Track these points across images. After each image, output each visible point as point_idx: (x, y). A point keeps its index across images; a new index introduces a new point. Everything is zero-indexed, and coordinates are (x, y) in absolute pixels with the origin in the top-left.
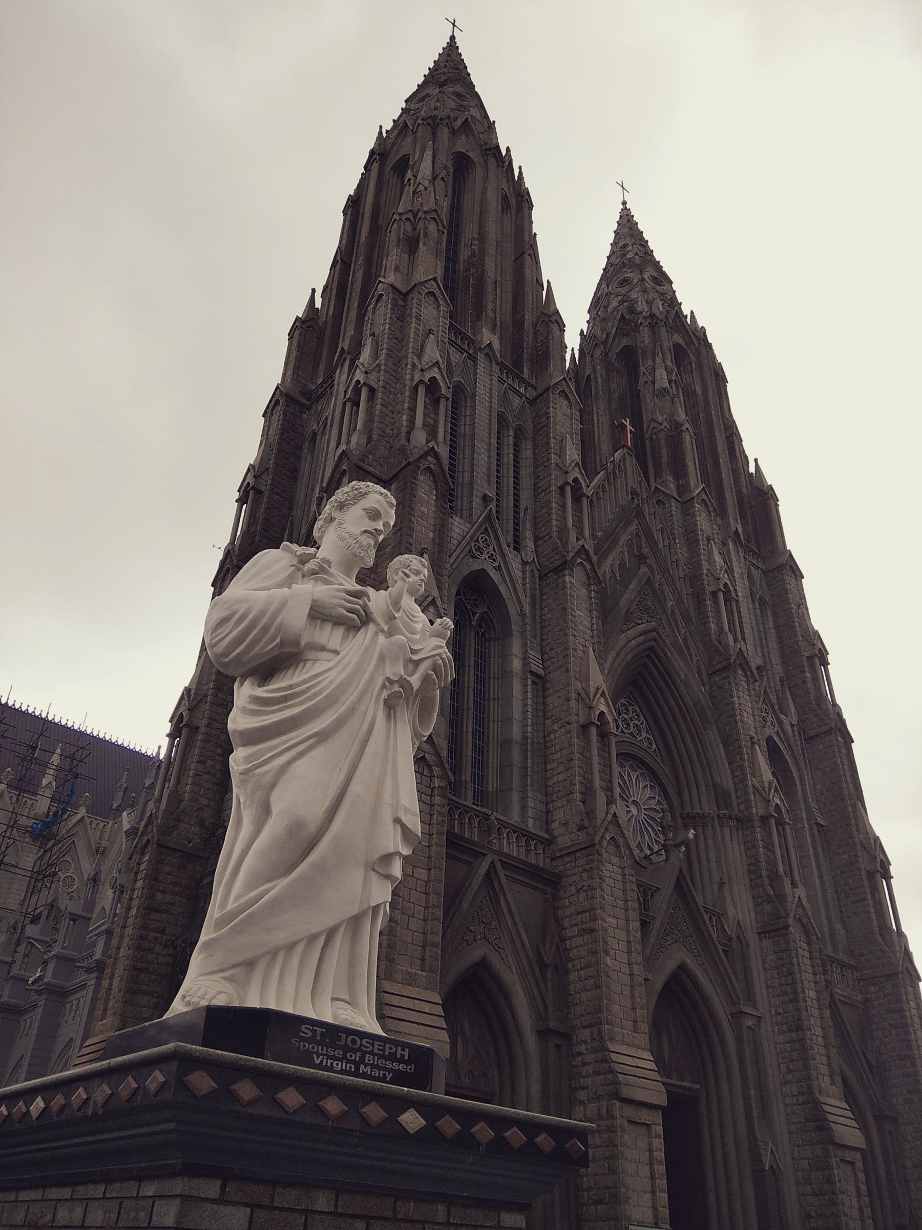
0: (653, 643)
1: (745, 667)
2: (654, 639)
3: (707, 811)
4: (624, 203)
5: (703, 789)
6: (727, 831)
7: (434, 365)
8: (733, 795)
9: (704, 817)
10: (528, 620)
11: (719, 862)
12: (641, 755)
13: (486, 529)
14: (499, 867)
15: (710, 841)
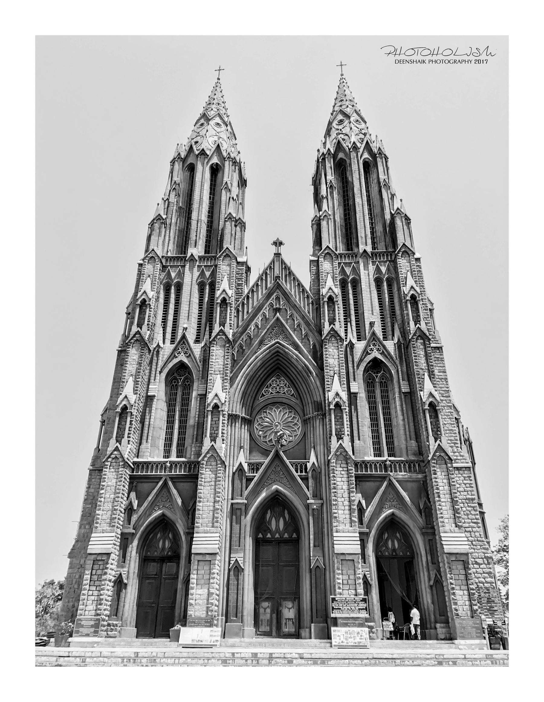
0: (278, 349)
1: (336, 335)
2: (278, 347)
3: (311, 415)
4: (342, 75)
5: (310, 405)
6: (318, 421)
7: (143, 293)
8: (323, 403)
9: (309, 418)
10: (201, 372)
11: (314, 437)
12: (280, 400)
13: (184, 342)
14: (168, 480)
15: (312, 428)
